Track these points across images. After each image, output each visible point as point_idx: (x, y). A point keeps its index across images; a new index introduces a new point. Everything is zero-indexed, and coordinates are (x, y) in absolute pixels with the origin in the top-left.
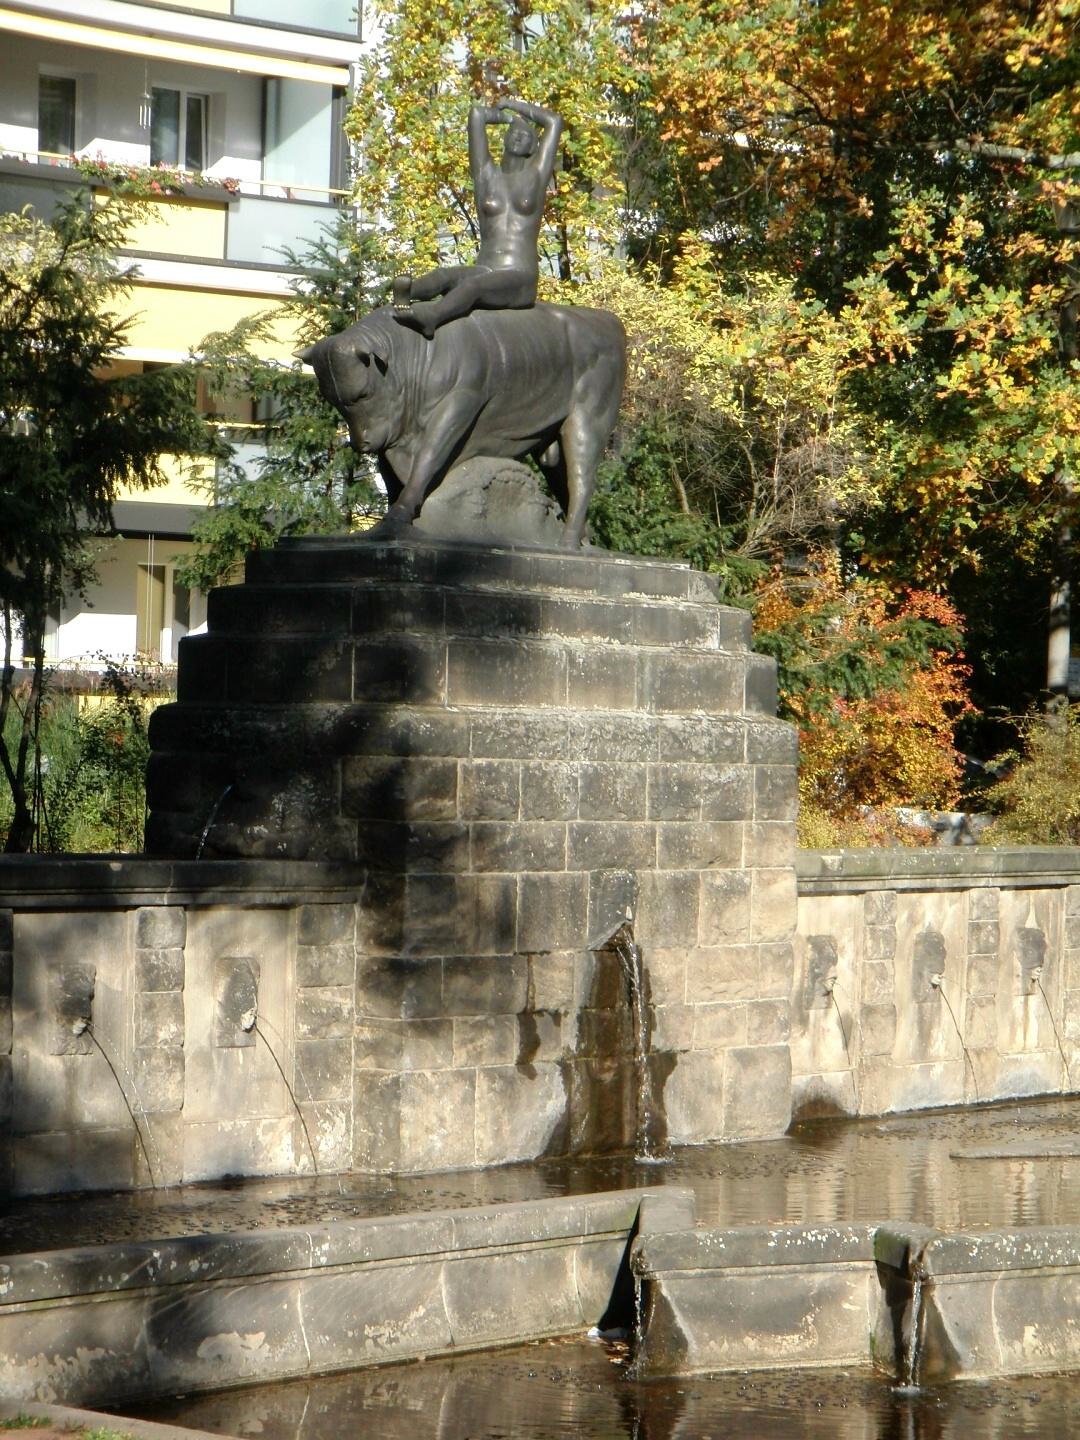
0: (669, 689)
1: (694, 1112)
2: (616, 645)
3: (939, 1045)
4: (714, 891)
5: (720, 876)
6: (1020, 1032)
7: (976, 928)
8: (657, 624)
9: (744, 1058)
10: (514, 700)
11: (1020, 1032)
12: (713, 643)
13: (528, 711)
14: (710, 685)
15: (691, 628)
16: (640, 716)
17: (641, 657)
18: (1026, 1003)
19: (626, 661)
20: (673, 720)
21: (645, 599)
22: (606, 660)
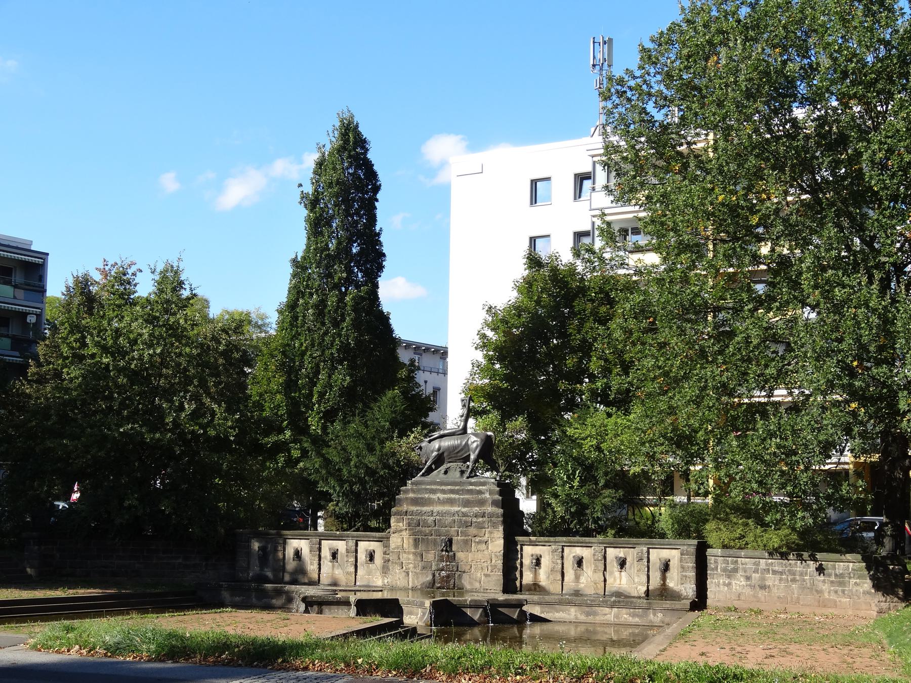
0: (467, 503)
1: (471, 583)
2: (457, 496)
3: (583, 580)
5: (477, 539)
7: (594, 555)
8: (470, 492)
9: (486, 575)
12: (487, 495)
13: (425, 509)
14: (482, 503)
15: (480, 492)
16: (456, 509)
17: (459, 498)
18: (620, 574)
19: (455, 499)
20: (465, 510)
21: (473, 487)
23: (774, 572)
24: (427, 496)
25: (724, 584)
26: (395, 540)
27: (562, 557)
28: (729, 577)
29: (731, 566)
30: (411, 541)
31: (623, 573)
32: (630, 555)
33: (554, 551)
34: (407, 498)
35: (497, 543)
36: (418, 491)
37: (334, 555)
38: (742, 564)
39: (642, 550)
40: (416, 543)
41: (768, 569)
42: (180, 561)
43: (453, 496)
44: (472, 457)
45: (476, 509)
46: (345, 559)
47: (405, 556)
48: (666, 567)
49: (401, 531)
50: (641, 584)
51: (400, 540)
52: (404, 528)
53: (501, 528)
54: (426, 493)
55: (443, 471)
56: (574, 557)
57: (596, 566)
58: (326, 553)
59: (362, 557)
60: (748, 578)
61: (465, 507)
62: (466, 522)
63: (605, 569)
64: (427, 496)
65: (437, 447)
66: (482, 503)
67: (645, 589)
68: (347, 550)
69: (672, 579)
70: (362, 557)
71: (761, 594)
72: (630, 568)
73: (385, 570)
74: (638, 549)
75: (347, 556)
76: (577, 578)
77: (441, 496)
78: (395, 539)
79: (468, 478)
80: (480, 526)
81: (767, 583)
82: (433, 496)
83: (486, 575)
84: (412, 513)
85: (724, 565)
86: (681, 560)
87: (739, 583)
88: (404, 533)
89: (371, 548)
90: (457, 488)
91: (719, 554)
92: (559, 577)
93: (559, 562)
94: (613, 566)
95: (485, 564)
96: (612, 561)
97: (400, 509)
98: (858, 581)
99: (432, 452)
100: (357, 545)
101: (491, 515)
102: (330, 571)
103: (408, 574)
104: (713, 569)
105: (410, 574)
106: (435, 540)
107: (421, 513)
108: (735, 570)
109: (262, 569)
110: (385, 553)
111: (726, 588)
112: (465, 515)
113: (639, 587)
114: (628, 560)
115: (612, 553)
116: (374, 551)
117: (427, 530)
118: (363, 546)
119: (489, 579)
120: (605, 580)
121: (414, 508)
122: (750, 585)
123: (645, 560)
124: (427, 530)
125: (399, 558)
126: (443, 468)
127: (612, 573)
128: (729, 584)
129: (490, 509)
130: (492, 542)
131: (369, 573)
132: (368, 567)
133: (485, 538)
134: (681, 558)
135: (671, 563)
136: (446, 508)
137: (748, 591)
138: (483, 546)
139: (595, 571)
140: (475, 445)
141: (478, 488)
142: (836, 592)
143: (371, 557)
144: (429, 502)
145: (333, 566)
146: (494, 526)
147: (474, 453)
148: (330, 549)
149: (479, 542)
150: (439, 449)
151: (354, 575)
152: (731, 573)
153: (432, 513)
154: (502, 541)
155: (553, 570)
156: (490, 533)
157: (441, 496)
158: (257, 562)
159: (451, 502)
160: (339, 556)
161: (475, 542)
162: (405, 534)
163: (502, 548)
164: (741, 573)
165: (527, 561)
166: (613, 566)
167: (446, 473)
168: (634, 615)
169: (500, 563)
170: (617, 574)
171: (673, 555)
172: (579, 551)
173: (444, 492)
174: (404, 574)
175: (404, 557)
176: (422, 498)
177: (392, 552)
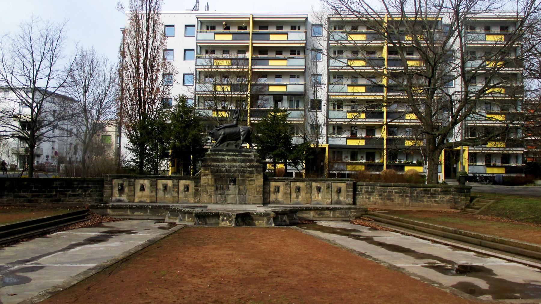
0: (244, 161)
3: (300, 197)
4: (248, 180)
5: (249, 179)
6: (317, 197)
8: (244, 155)
9: (254, 197)
10: (219, 162)
11: (317, 197)
13: (220, 164)
15: (249, 156)
18: (318, 195)
20: (243, 164)
22: (234, 159)
23: (396, 193)
24: (220, 157)
25: (366, 198)
26: (203, 180)
27: (290, 187)
28: (369, 195)
29: (370, 190)
30: (213, 180)
31: (320, 194)
32: (323, 186)
33: (286, 184)
34: (210, 158)
35: (260, 181)
36: (217, 155)
37: (165, 187)
38: (377, 189)
39: (329, 183)
40: (216, 181)
41: (392, 192)
42: (70, 192)
43: (235, 157)
44: (242, 138)
45: (248, 164)
46: (172, 189)
47: (209, 187)
48: (339, 191)
49: (207, 175)
50: (329, 199)
51: (206, 180)
52: (209, 173)
53: (262, 174)
54: (220, 156)
55: (226, 145)
56: (296, 187)
57: (307, 191)
58: (160, 186)
59: (181, 188)
60: (380, 195)
61: (242, 163)
62: (243, 170)
63: (311, 193)
64: (220, 157)
65: (222, 133)
66: (251, 161)
67: (330, 201)
68: (173, 184)
69: (342, 196)
70: (181, 188)
71: (388, 202)
72: (323, 191)
73: (196, 193)
74: (327, 183)
75: (173, 188)
76: (297, 197)
77: (229, 158)
78: (204, 179)
79: (240, 148)
80: (251, 172)
81: (391, 197)
82: (223, 157)
83: (254, 197)
84: (213, 166)
85: (365, 190)
86: (347, 188)
87: (375, 198)
88: (209, 176)
89: (187, 184)
90: (236, 153)
91: (364, 185)
92: (289, 196)
93: (289, 189)
94: (314, 191)
95: (254, 191)
96: (314, 188)
97: (207, 164)
98: (443, 196)
99: (220, 135)
100: (178, 182)
101: (257, 167)
102: (163, 196)
103: (211, 196)
104: (359, 192)
105: (212, 196)
106: (226, 179)
107: (218, 166)
108: (373, 192)
109: (120, 196)
110: (196, 186)
111: (367, 200)
112: (242, 167)
113: (328, 200)
114: (322, 188)
115: (314, 184)
116: (189, 185)
117: (222, 174)
118: (182, 183)
119: (256, 198)
120: (311, 198)
121: (215, 164)
122: (381, 199)
123: (330, 188)
124: (222, 174)
125: (206, 189)
126: (226, 143)
127: (314, 194)
128: (369, 198)
129: (256, 164)
130: (257, 180)
131: (186, 196)
132: (185, 193)
133: (254, 178)
134: (347, 187)
135: (342, 189)
136: (232, 164)
137: (380, 201)
138: (253, 182)
139: (306, 193)
140: (242, 133)
141: (248, 153)
142: (431, 201)
143: (187, 188)
144: (223, 160)
145: (165, 193)
146: (259, 172)
147: (243, 136)
148: (163, 185)
149: (251, 180)
150: (224, 134)
151: (177, 198)
152: (370, 194)
153: (224, 166)
154: (262, 180)
155: (285, 193)
156: (256, 176)
157: (229, 158)
158: (117, 192)
159: (234, 161)
160: (168, 188)
161: (248, 180)
162: (210, 177)
163: (262, 183)
164: (376, 193)
165: (272, 189)
166: (314, 191)
167: (227, 146)
168: (341, 214)
169: (261, 190)
170: (316, 194)
171: (343, 185)
172: (298, 184)
173: (230, 155)
174: (209, 197)
175: (208, 188)
176: (218, 158)
177: (203, 186)
